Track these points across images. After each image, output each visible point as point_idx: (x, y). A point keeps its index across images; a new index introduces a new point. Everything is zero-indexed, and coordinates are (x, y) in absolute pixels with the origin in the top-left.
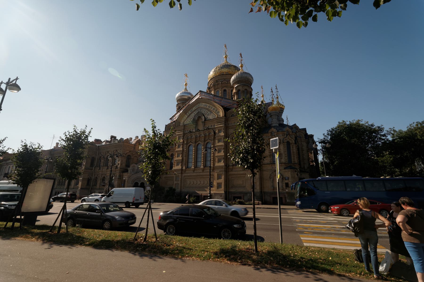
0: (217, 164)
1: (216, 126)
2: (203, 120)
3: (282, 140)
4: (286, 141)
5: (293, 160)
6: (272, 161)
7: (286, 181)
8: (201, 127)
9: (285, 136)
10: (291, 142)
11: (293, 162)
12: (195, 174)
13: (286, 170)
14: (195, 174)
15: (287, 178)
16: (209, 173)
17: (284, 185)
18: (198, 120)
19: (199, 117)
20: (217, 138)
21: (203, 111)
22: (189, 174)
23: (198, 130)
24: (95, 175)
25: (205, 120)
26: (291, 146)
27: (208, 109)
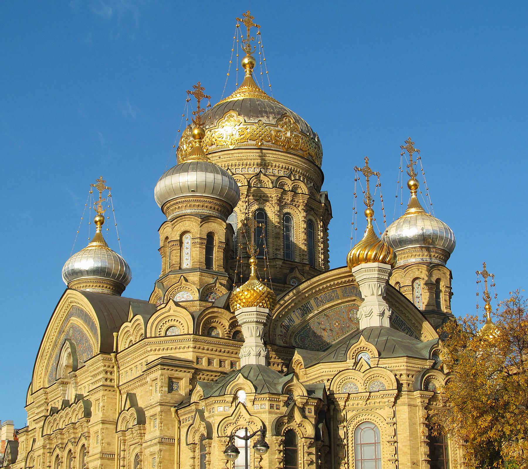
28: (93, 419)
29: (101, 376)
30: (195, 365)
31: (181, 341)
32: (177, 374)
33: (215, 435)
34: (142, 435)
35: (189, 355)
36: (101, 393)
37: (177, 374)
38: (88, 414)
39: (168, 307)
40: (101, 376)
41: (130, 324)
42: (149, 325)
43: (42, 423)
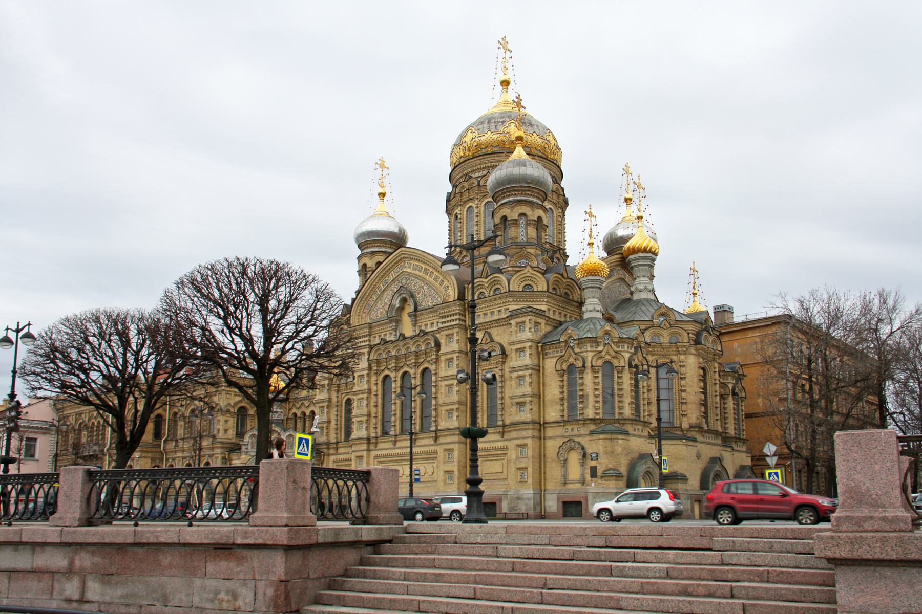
0: (443, 425)
1: (441, 325)
2: (412, 309)
3: (590, 359)
4: (600, 362)
5: (617, 411)
6: (565, 413)
7: (593, 463)
8: (408, 329)
9: (600, 348)
10: (615, 363)
11: (617, 416)
12: (397, 451)
13: (595, 437)
14: (397, 451)
15: (594, 455)
16: (408, 450)
17: (588, 471)
18: (401, 309)
19: (404, 301)
20: (443, 358)
21: (413, 285)
22: (384, 452)
23: (403, 337)
24: (167, 460)
25: (416, 310)
26: (615, 372)
27: (423, 280)
28: (443, 349)
29: (458, 317)
30: (547, 314)
31: (537, 296)
32: (539, 320)
33: (588, 365)
34: (503, 363)
35: (544, 308)
36: (455, 330)
37: (539, 320)
38: (438, 345)
39: (526, 270)
40: (458, 317)
41: (485, 281)
42: (511, 282)
43: (367, 350)
